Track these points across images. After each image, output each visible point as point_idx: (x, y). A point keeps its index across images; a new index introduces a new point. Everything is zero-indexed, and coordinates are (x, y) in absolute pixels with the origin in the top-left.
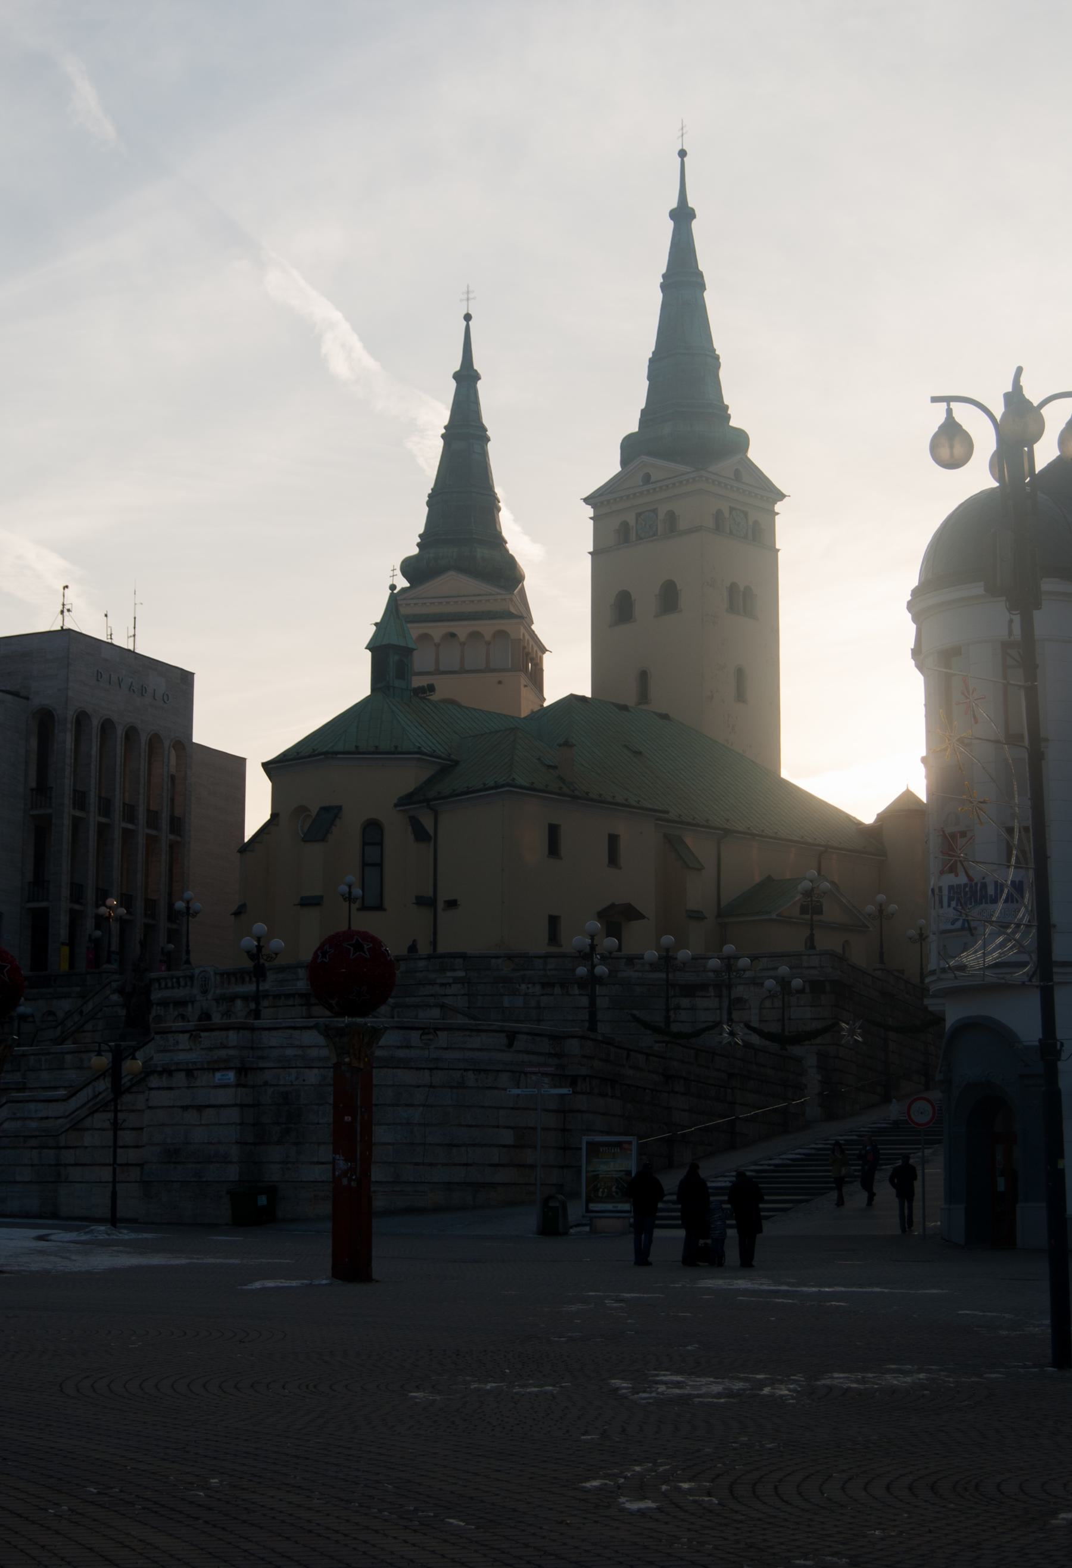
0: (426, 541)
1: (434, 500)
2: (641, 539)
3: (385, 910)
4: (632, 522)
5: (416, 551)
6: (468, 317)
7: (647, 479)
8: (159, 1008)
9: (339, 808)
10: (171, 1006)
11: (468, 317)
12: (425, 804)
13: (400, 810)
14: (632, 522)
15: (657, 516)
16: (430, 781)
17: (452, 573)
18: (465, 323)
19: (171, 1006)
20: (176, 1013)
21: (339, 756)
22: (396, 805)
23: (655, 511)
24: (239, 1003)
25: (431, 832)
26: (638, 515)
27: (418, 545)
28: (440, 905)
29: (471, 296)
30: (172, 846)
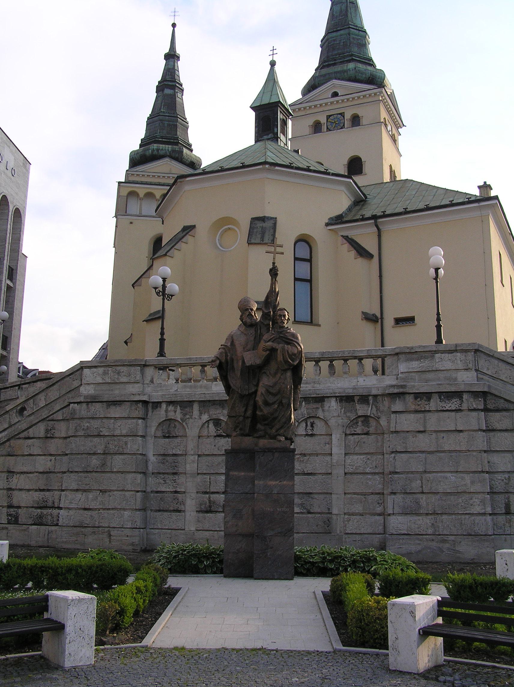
0: (144, 143)
1: (151, 121)
2: (330, 130)
3: (320, 326)
4: (323, 120)
5: (137, 148)
6: (174, 25)
7: (335, 94)
8: (171, 408)
9: (276, 218)
10: (196, 406)
11: (174, 25)
12: (373, 221)
13: (330, 230)
14: (323, 120)
15: (344, 117)
16: (350, 209)
17: (167, 159)
18: (172, 28)
19: (196, 406)
20: (205, 417)
21: (277, 168)
22: (327, 225)
23: (342, 114)
24: (333, 404)
25: (373, 250)
26: (328, 117)
27: (141, 146)
28: (389, 322)
29: (176, 14)
30: (9, 288)
